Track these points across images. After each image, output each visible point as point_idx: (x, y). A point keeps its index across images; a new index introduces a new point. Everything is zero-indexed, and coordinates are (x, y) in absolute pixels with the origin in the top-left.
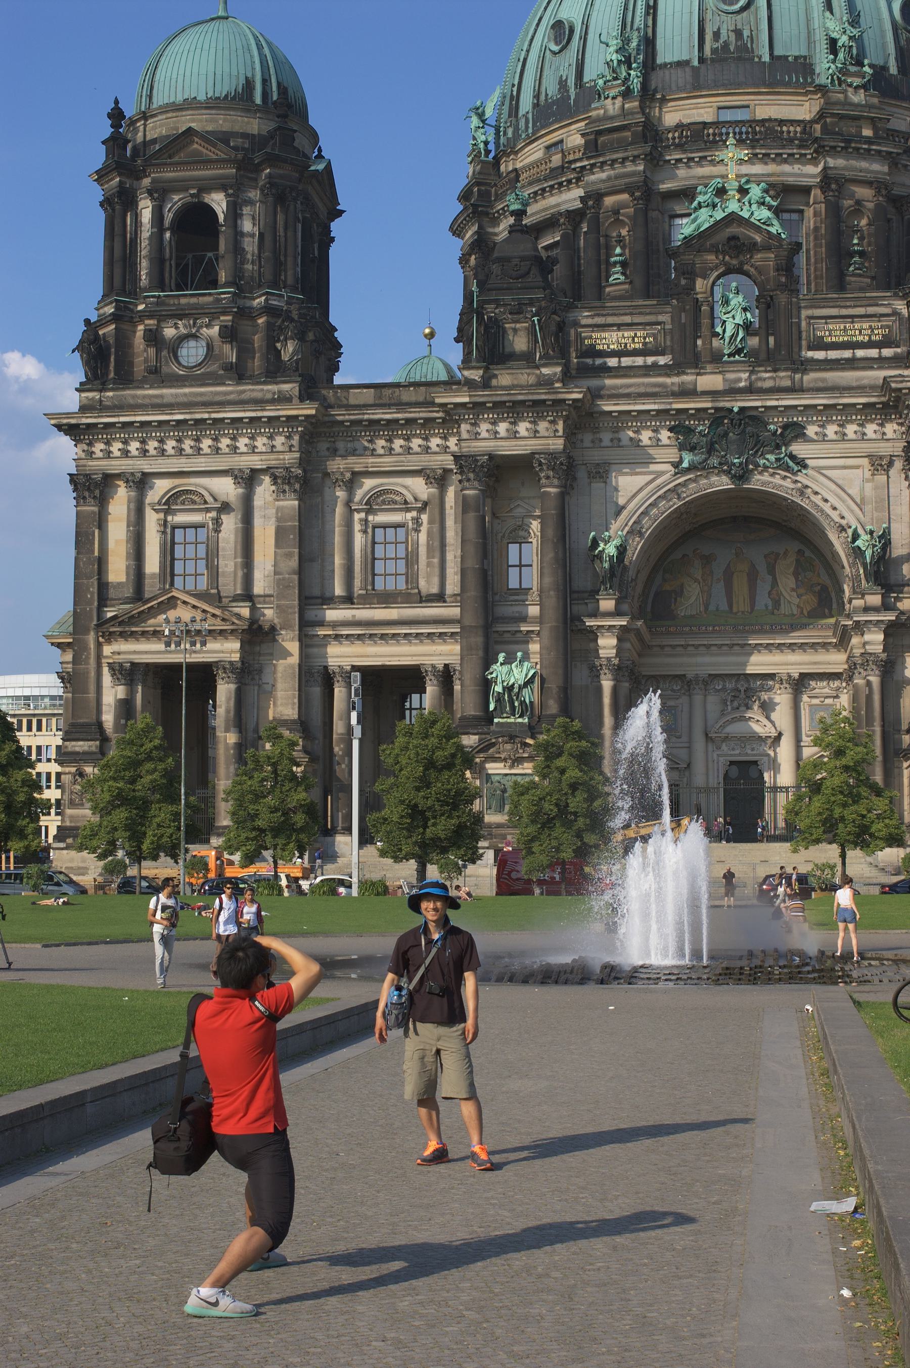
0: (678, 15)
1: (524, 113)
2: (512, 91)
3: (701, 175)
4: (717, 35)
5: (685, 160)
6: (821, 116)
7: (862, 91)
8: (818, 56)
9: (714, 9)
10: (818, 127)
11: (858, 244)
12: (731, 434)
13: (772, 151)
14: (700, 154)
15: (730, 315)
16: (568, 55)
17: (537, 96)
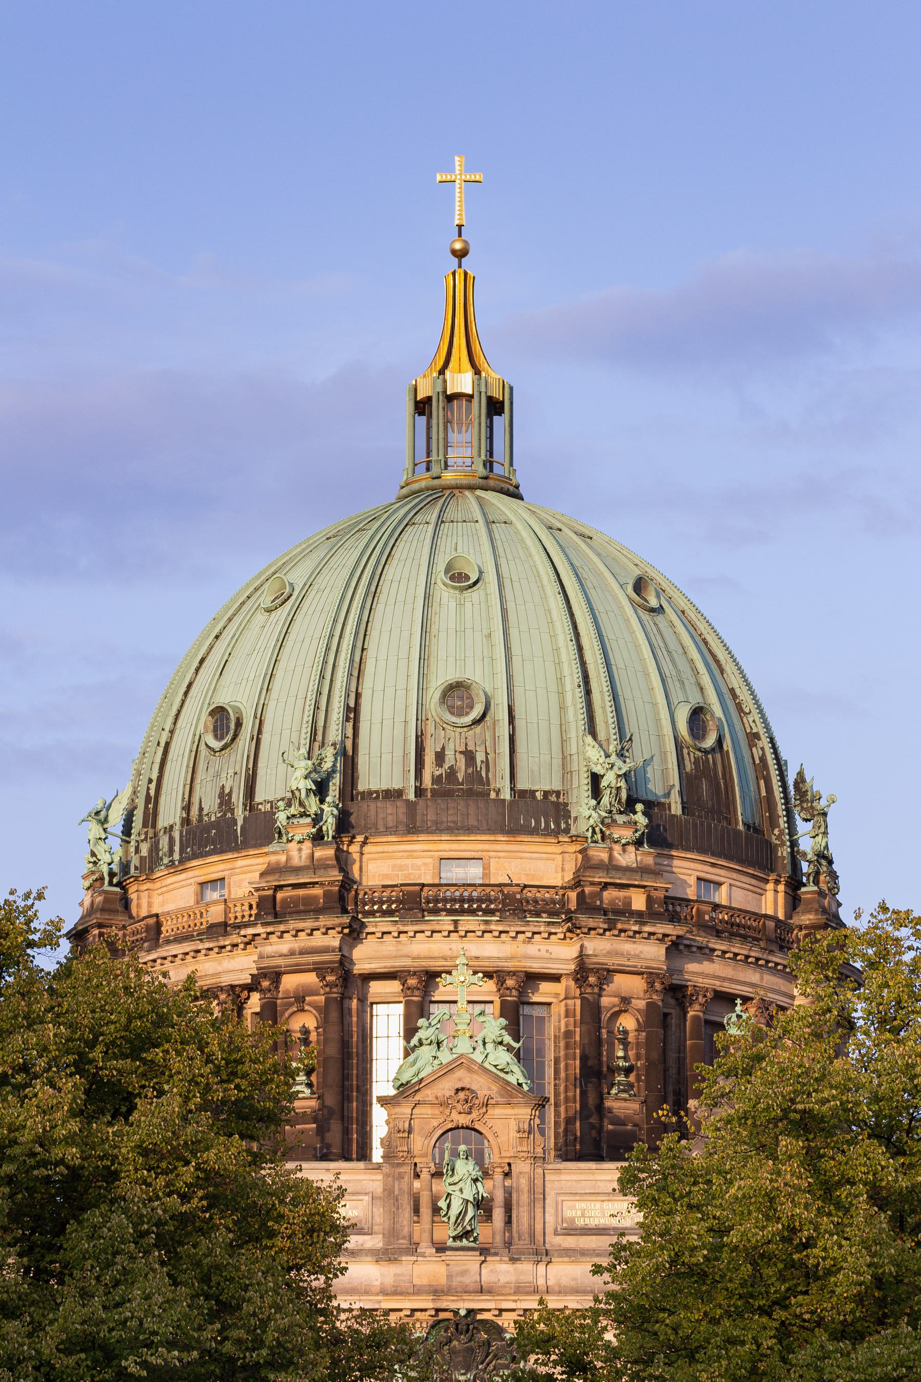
0: (387, 723)
1: (166, 825)
2: (148, 789)
3: (415, 954)
4: (440, 757)
5: (396, 934)
6: (577, 883)
7: (631, 849)
8: (575, 792)
9: (438, 720)
10: (573, 895)
11: (625, 1058)
12: (455, 1343)
13: (512, 929)
14: (417, 928)
15: (457, 1188)
16: (233, 758)
17: (187, 808)
